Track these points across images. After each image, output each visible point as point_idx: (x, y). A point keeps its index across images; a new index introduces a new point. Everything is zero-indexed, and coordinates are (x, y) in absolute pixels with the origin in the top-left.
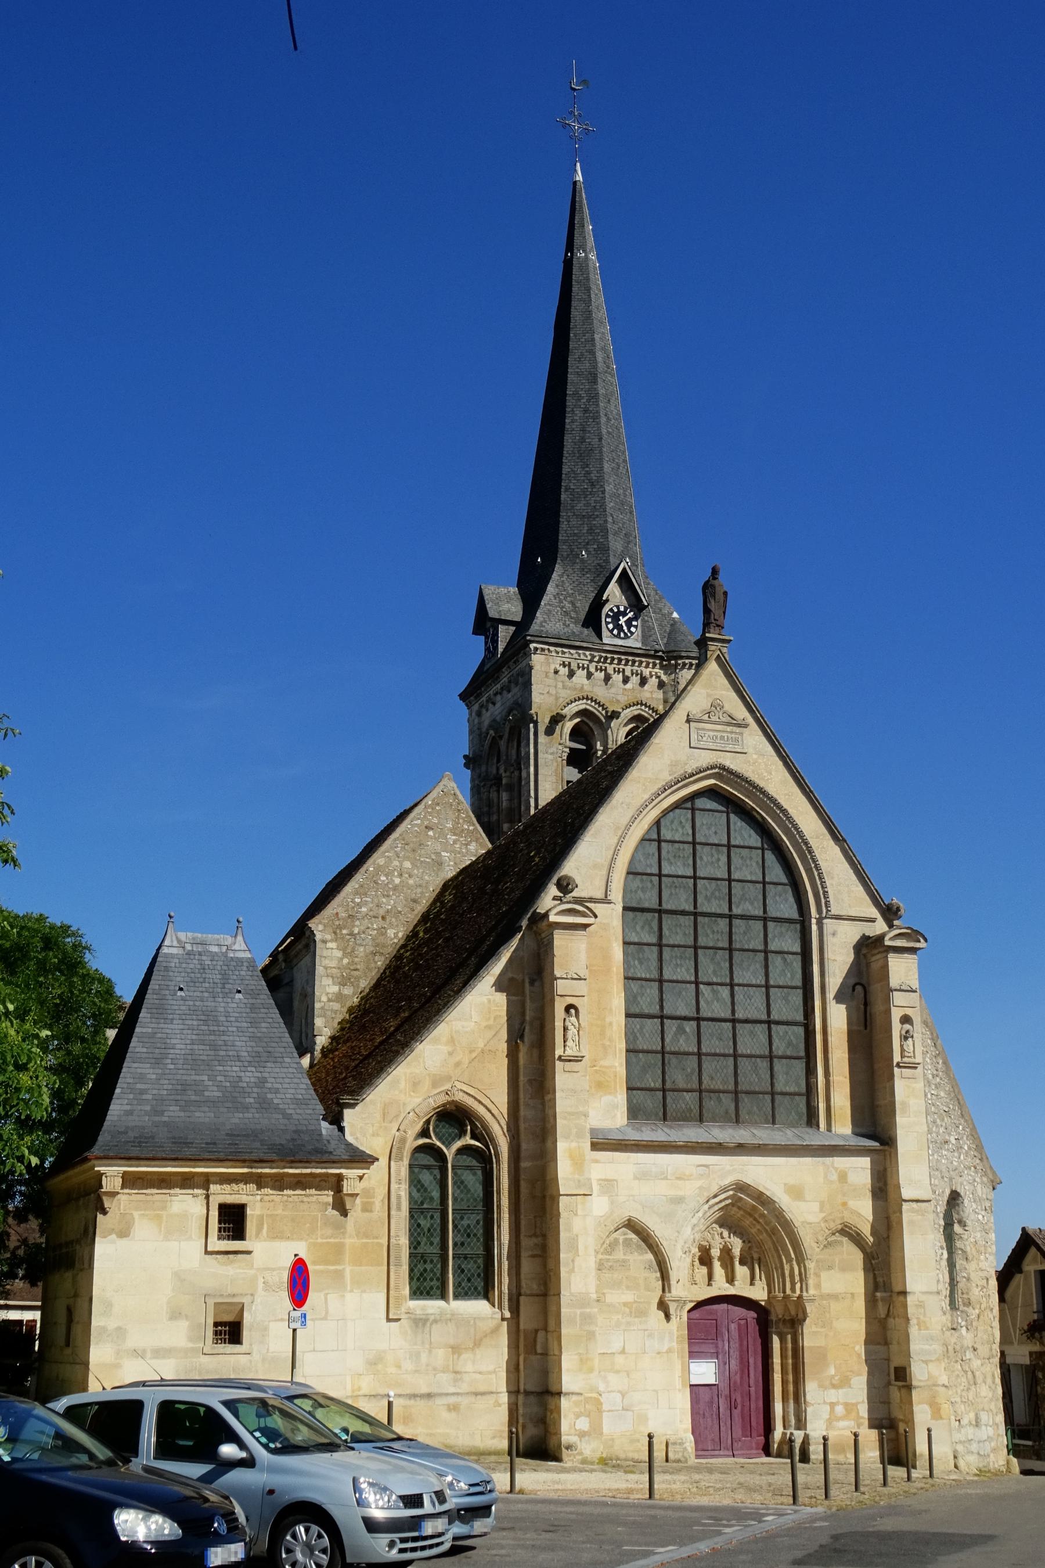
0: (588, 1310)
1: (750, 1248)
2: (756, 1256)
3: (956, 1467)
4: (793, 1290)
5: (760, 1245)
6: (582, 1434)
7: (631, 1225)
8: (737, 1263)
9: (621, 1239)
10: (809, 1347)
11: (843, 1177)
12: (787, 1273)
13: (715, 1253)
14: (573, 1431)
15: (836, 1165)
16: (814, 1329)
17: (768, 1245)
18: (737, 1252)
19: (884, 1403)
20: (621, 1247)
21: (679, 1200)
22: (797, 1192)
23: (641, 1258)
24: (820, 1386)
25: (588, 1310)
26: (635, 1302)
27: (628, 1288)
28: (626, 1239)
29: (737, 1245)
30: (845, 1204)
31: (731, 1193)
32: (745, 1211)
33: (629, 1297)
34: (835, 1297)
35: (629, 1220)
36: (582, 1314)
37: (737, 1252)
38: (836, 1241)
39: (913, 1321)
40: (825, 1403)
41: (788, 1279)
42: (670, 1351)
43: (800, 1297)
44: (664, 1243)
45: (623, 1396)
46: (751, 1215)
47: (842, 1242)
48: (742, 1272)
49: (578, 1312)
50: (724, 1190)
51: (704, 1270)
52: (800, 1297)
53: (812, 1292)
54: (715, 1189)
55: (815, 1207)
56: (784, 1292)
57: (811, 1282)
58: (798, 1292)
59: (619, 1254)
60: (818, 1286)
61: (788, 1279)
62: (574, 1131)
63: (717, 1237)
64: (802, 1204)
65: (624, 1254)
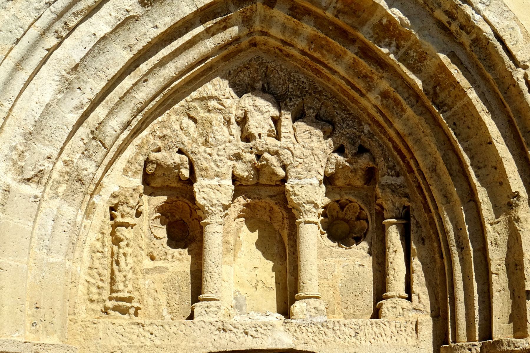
1: (370, 175)
2: (388, 201)
5: (402, 159)
8: (312, 237)
12: (497, 256)
13: (213, 191)
17: (427, 154)
18: (309, 192)
29: (308, 159)
32: (320, 22)
37: (309, 192)
41: (500, 282)
46: (346, 37)
51: (180, 261)
56: (487, 332)
61: (500, 282)
63: (227, 137)
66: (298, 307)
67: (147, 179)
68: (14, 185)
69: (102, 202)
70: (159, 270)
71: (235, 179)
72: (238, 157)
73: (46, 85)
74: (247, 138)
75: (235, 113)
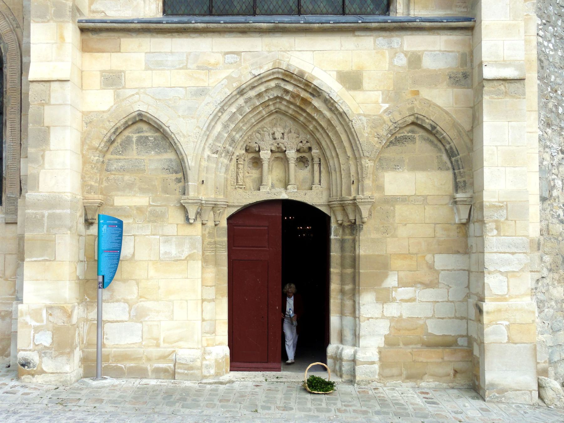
0: (58, 211)
3: (540, 397)
4: (350, 194)
6: (43, 352)
7: (141, 119)
9: (135, 137)
10: (366, 257)
11: (415, 60)
13: (265, 155)
14: (31, 347)
15: (405, 48)
16: (374, 235)
18: (292, 154)
19: (462, 318)
20: (135, 147)
21: (201, 92)
22: (352, 80)
23: (158, 157)
24: (378, 300)
25: (58, 211)
26: (150, 205)
27: (143, 191)
28: (141, 137)
30: (417, 93)
31: (273, 84)
33: (142, 200)
34: (404, 199)
35: (140, 115)
36: (50, 216)
38: (405, 138)
39: (490, 225)
40: (383, 317)
42: (190, 257)
43: (355, 199)
44: (182, 140)
45: (130, 306)
47: (414, 138)
48: (298, 174)
49: (46, 213)
50: (260, 80)
52: (355, 199)
53: (367, 194)
54: (247, 79)
55: (377, 96)
57: (368, 182)
58: (353, 194)
59: (133, 153)
60: (380, 188)
62: (52, 10)
64: (359, 95)
65: (138, 154)
66: (289, 187)
67: (247, 150)
68: (210, 154)
69: (234, 158)
70: (250, 176)
71: (271, 151)
72: (272, 144)
73: (219, 127)
74: (275, 139)
75: (271, 132)
